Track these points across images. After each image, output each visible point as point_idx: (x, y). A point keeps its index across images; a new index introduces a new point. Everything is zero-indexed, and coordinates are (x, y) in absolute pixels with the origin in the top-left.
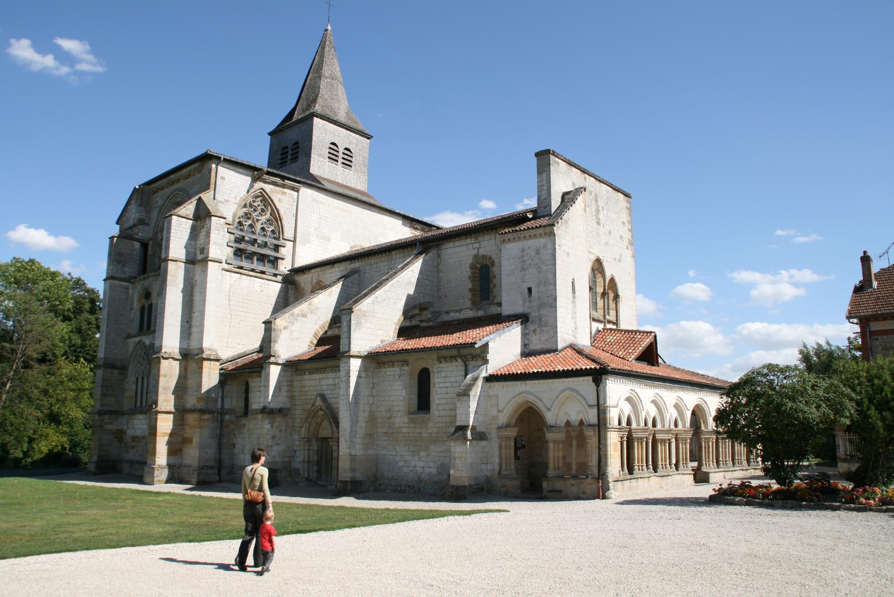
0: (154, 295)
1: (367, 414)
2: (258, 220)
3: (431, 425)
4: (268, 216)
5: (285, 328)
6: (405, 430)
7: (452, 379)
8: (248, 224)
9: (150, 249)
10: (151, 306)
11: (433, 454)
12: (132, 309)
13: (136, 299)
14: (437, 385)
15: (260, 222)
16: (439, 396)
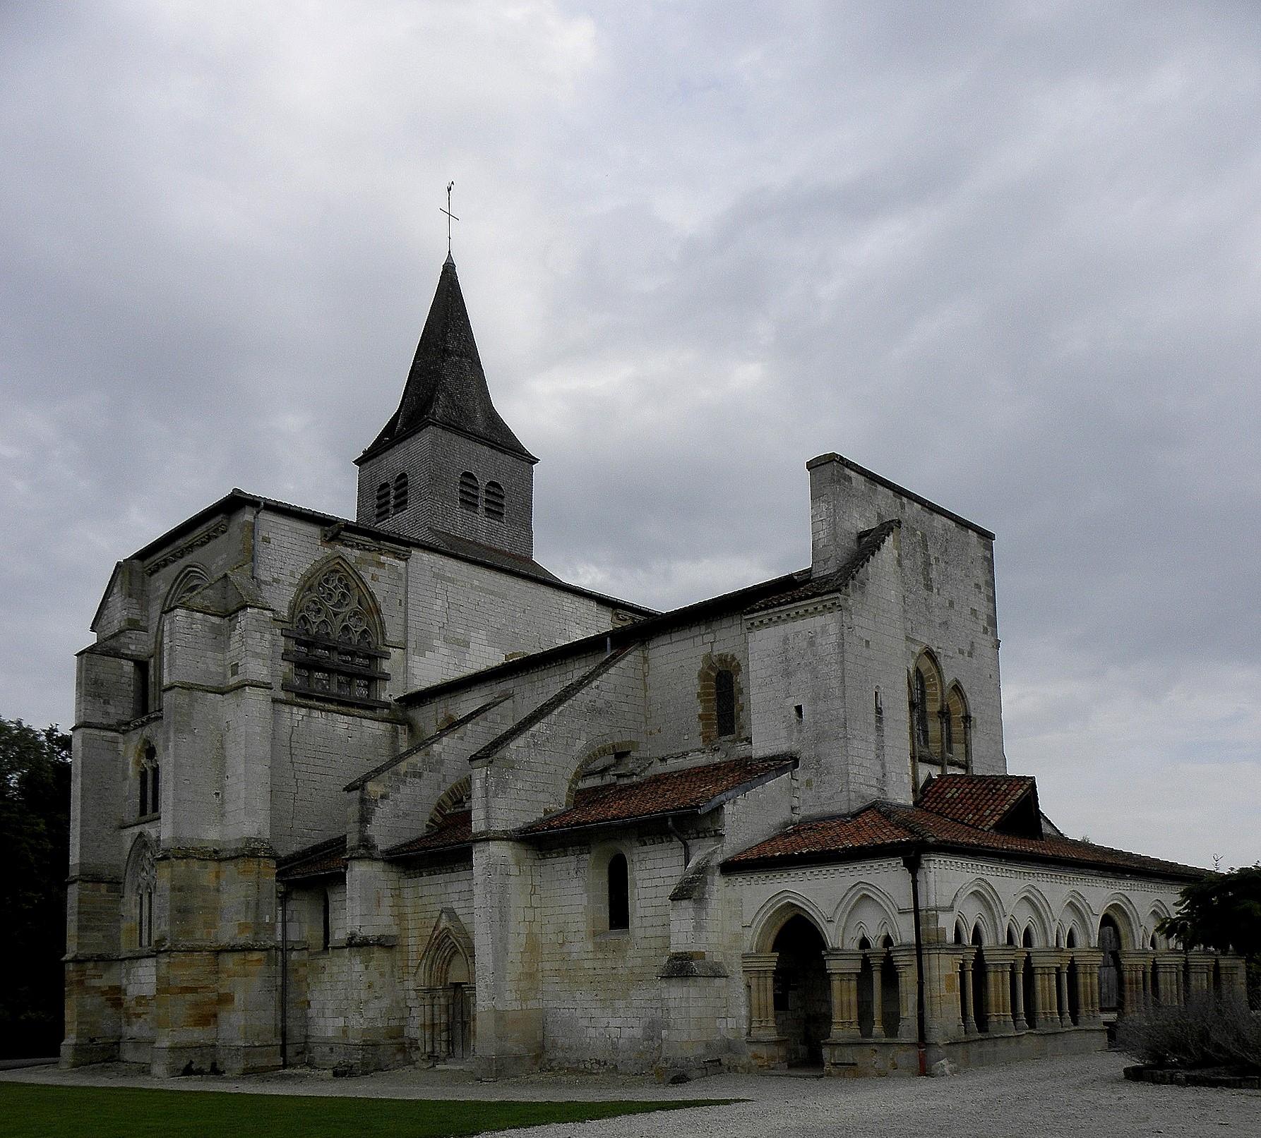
0: (159, 750)
1: (523, 939)
2: (336, 614)
3: (630, 953)
4: (355, 604)
5: (383, 797)
6: (587, 965)
7: (664, 873)
8: (318, 621)
9: (151, 672)
10: (156, 771)
11: (636, 1003)
12: (125, 779)
13: (131, 760)
14: (639, 884)
15: (341, 617)
16: (643, 903)
